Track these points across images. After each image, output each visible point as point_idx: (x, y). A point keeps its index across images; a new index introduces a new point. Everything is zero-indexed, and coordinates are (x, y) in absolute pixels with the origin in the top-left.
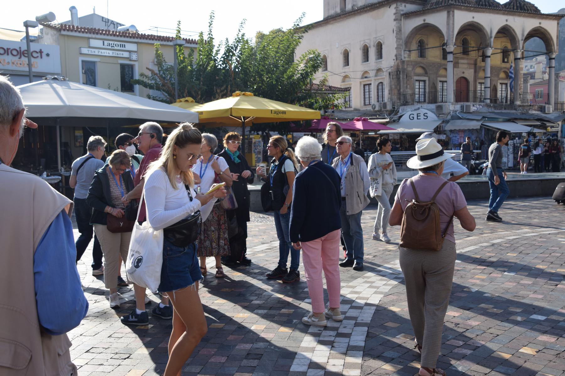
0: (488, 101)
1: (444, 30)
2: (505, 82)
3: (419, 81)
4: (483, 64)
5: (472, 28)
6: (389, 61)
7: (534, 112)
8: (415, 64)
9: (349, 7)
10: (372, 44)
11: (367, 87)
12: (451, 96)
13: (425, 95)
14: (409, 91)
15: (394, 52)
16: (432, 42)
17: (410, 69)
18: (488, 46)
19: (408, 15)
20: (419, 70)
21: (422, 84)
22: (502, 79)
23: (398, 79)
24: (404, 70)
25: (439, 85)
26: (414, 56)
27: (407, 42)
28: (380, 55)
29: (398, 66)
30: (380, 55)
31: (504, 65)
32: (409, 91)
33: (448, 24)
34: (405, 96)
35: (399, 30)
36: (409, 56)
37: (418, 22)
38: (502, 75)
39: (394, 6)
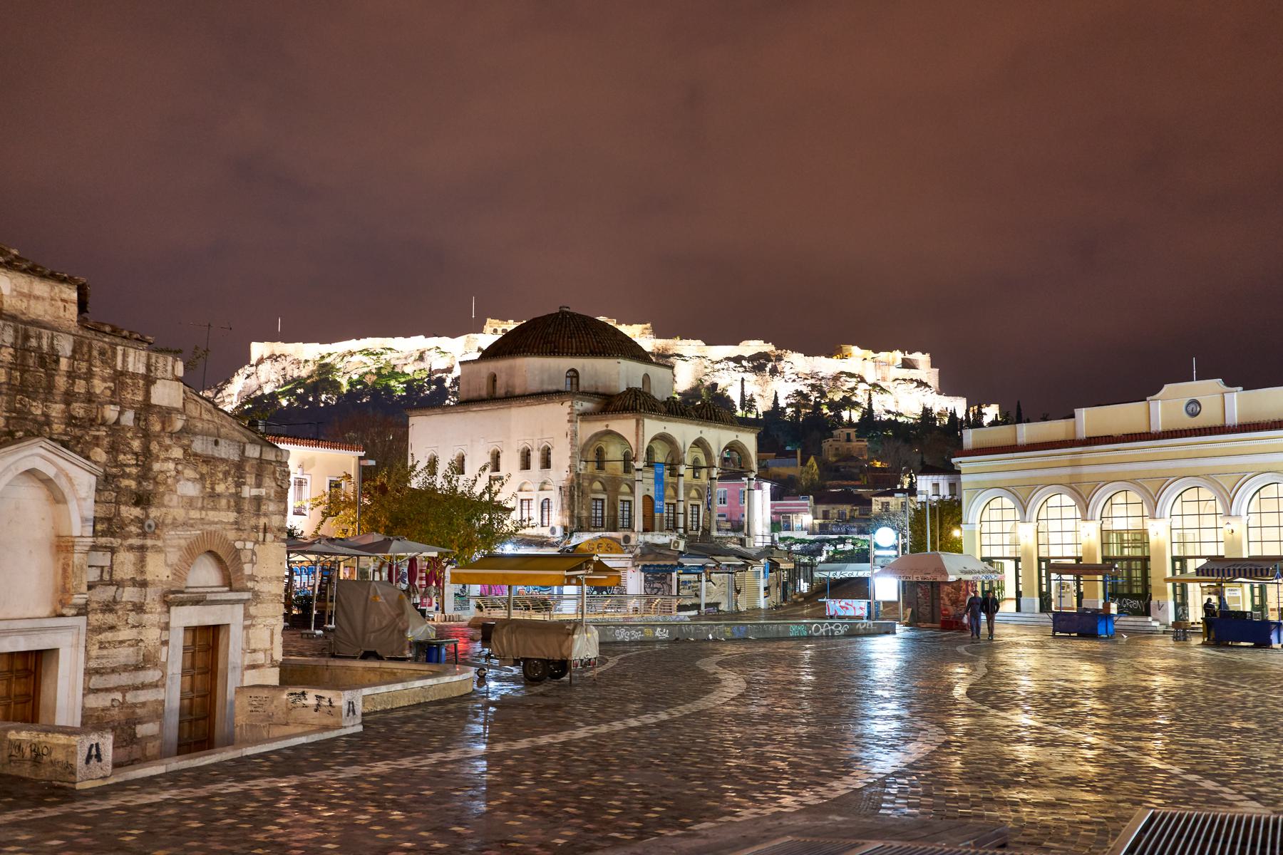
0: (681, 531)
1: (632, 442)
2: (699, 502)
3: (596, 500)
4: (671, 480)
5: (664, 438)
6: (560, 473)
7: (733, 546)
8: (593, 479)
9: (501, 391)
10: (535, 447)
11: (525, 504)
12: (639, 523)
13: (603, 517)
14: (585, 514)
15: (568, 462)
16: (614, 452)
17: (586, 484)
18: (681, 462)
19: (585, 416)
20: (597, 486)
21: (599, 504)
22: (693, 499)
23: (572, 497)
24: (579, 484)
25: (620, 505)
26: (591, 467)
27: (584, 450)
28: (546, 464)
29: (572, 481)
30: (546, 464)
31: (695, 482)
32: (585, 514)
33: (637, 435)
34: (579, 519)
35: (575, 434)
36: (586, 468)
37: (599, 427)
38: (694, 494)
39: (569, 403)
